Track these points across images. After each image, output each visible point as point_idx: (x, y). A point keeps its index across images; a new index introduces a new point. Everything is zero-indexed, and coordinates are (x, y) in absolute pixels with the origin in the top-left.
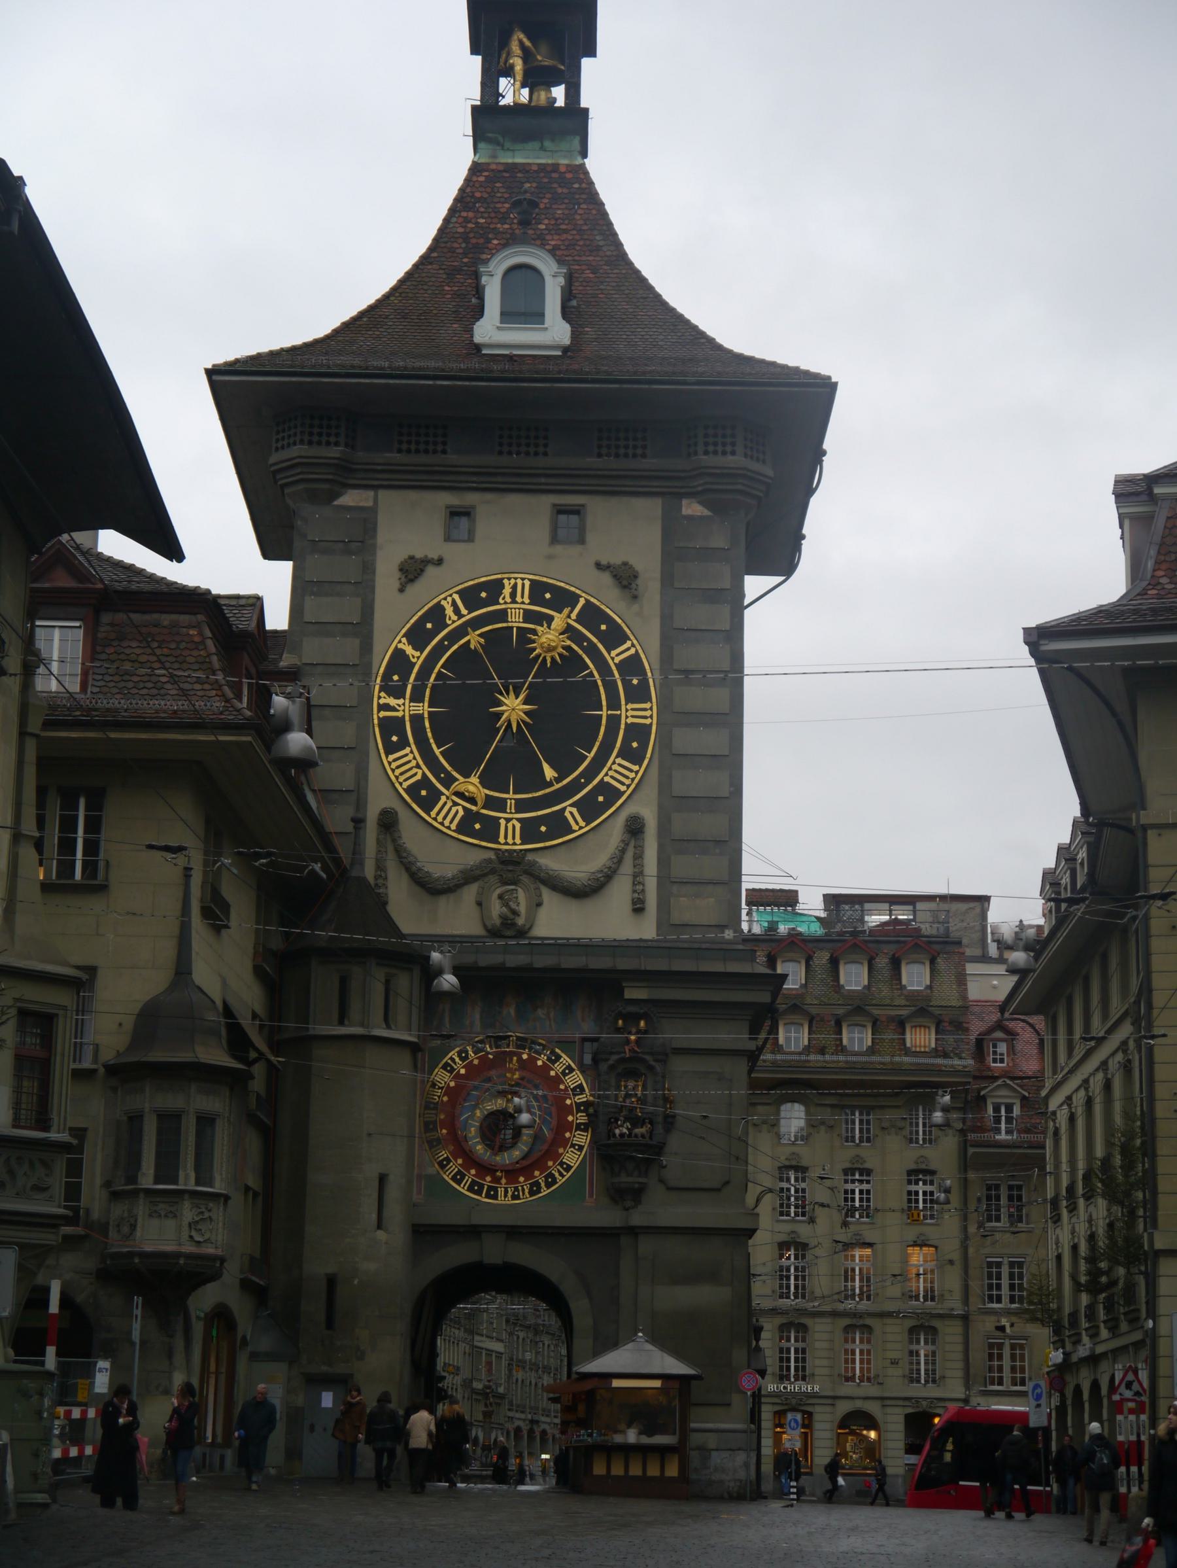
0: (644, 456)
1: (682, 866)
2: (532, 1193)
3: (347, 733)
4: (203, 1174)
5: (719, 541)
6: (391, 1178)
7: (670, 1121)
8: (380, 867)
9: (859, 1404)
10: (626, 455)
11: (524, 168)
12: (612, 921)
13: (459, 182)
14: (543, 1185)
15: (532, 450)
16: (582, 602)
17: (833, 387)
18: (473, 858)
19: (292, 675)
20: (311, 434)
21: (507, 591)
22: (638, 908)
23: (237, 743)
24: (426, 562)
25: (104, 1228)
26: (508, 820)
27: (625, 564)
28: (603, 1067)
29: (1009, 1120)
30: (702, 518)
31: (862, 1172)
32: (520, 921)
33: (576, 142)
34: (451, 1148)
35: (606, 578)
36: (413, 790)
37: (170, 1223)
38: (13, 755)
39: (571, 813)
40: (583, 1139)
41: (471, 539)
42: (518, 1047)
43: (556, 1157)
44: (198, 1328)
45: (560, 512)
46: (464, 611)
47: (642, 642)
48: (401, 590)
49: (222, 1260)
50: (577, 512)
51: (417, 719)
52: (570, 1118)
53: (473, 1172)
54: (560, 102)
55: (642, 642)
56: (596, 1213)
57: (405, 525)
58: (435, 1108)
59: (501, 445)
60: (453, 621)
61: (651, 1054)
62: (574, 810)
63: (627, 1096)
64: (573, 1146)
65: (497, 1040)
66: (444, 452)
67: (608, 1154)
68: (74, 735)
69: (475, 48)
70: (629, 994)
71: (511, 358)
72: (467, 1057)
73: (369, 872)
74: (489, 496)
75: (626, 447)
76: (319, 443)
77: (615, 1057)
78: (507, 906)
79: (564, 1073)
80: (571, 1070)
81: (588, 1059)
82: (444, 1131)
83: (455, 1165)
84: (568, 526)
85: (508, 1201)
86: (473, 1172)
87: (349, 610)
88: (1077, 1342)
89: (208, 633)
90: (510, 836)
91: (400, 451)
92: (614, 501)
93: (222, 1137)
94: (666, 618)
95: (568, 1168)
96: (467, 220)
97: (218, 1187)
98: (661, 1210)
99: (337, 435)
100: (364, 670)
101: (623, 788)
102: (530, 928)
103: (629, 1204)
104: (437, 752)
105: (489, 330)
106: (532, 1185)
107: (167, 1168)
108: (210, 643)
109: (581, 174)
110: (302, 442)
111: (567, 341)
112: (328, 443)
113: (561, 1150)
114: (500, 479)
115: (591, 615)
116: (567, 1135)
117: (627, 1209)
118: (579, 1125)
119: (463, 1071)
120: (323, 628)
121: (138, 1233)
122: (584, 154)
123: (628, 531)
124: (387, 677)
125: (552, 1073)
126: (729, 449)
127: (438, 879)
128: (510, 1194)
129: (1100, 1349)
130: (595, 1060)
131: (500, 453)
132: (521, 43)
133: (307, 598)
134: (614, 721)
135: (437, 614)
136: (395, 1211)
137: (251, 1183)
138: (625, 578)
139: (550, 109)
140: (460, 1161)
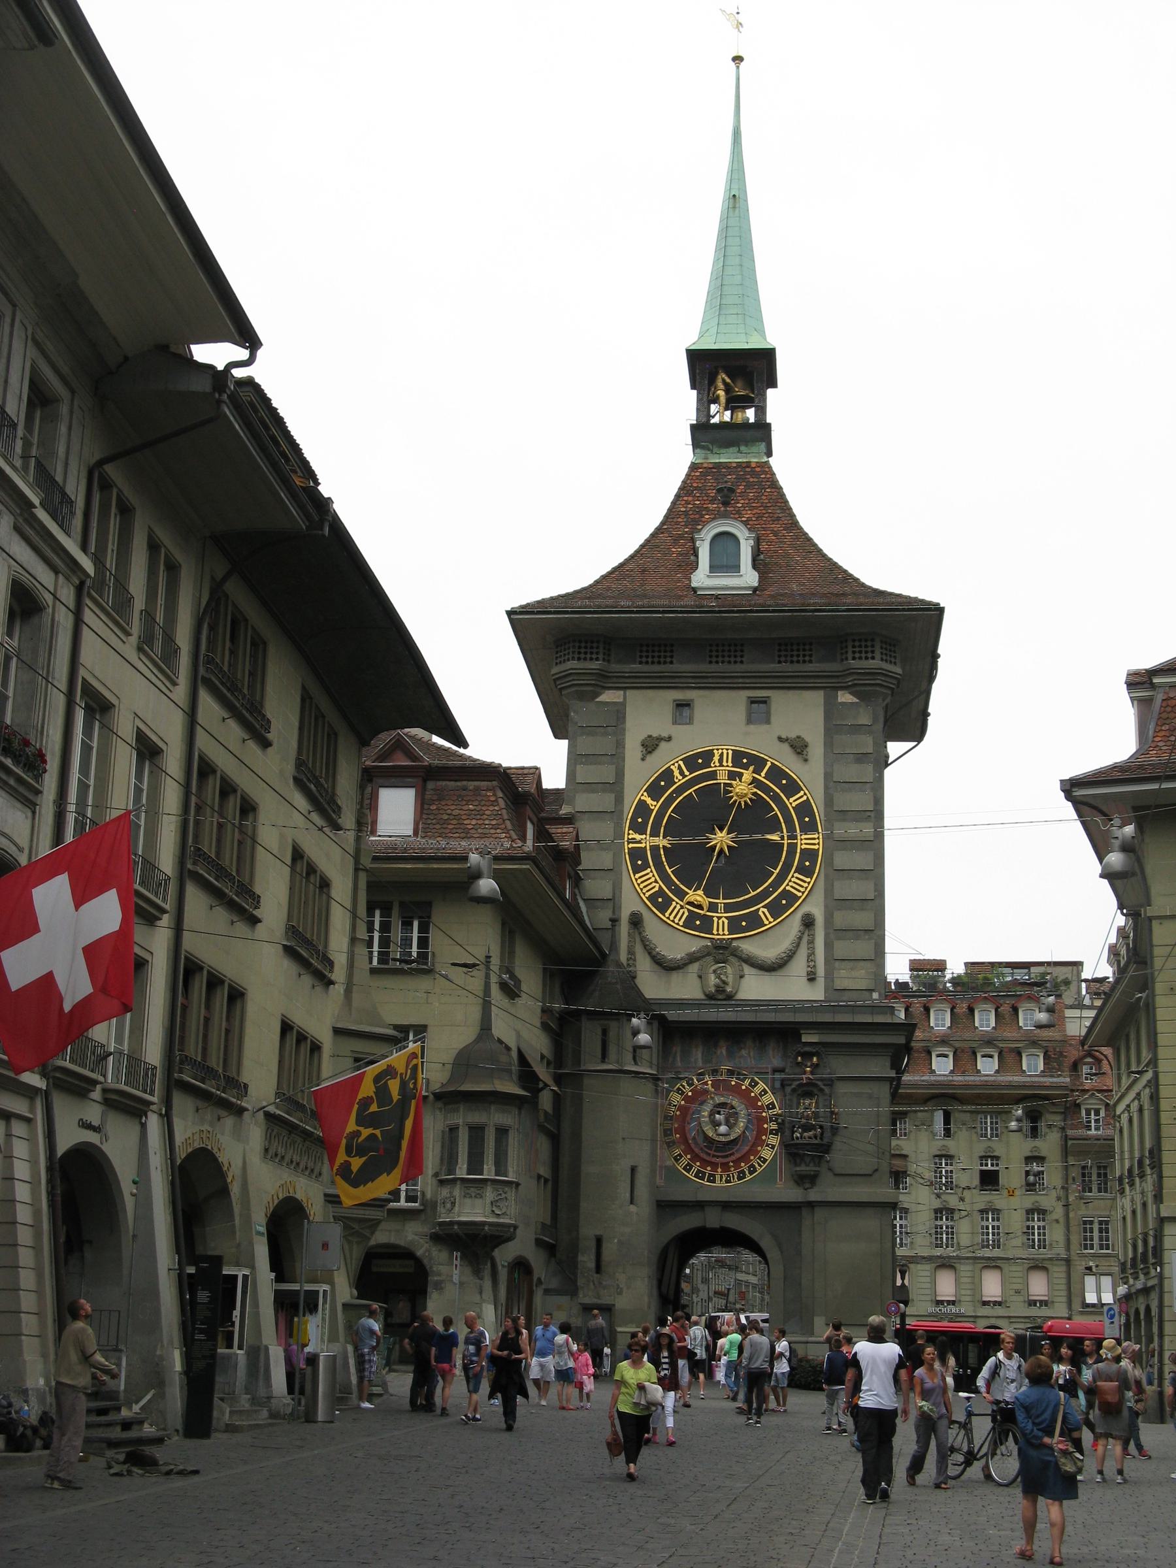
0: (810, 662)
1: (843, 948)
3: (606, 860)
4: (500, 1166)
5: (864, 719)
6: (640, 1169)
8: (631, 952)
9: (993, 1322)
10: (798, 662)
11: (726, 466)
12: (794, 988)
13: (682, 477)
15: (732, 659)
16: (769, 764)
17: (941, 611)
18: (694, 946)
19: (569, 820)
20: (579, 653)
21: (716, 758)
22: (812, 978)
23: (520, 870)
24: (660, 739)
25: (434, 1205)
26: (719, 918)
27: (799, 737)
28: (788, 1089)
29: (1097, 1121)
30: (852, 703)
31: (993, 1158)
32: (729, 989)
33: (763, 446)
35: (786, 746)
36: (652, 898)
37: (478, 1202)
38: (350, 885)
39: (763, 912)
40: (774, 1140)
41: (690, 721)
44: (503, 1275)
45: (752, 702)
46: (687, 773)
47: (812, 790)
48: (643, 759)
49: (515, 1227)
50: (765, 702)
51: (655, 849)
54: (752, 420)
55: (812, 790)
56: (784, 1191)
57: (646, 714)
59: (711, 656)
60: (679, 780)
62: (765, 910)
65: (715, 1072)
66: (671, 663)
67: (792, 1151)
68: (409, 866)
69: (693, 387)
71: (717, 597)
73: (623, 957)
74: (701, 692)
75: (798, 656)
76: (585, 659)
78: (719, 978)
80: (766, 1092)
81: (777, 1085)
84: (759, 711)
85: (722, 1185)
87: (606, 773)
88: (1136, 1278)
89: (500, 794)
90: (721, 929)
91: (641, 663)
92: (791, 693)
93: (513, 1141)
94: (828, 776)
96: (688, 503)
97: (511, 1178)
98: (829, 1190)
99: (597, 653)
100: (616, 814)
101: (799, 894)
103: (807, 1185)
104: (669, 871)
105: (702, 578)
107: (475, 1165)
108: (501, 802)
109: (766, 469)
110: (573, 659)
111: (756, 584)
112: (591, 659)
114: (710, 680)
115: (776, 774)
120: (589, 787)
121: (456, 1209)
122: (769, 454)
123: (800, 713)
124: (634, 819)
126: (870, 655)
127: (671, 960)
129: (1150, 1284)
130: (783, 1086)
131: (711, 662)
132: (724, 380)
133: (578, 767)
134: (792, 848)
135: (668, 775)
136: (642, 1191)
137: (542, 1173)
138: (799, 747)
139: (746, 425)
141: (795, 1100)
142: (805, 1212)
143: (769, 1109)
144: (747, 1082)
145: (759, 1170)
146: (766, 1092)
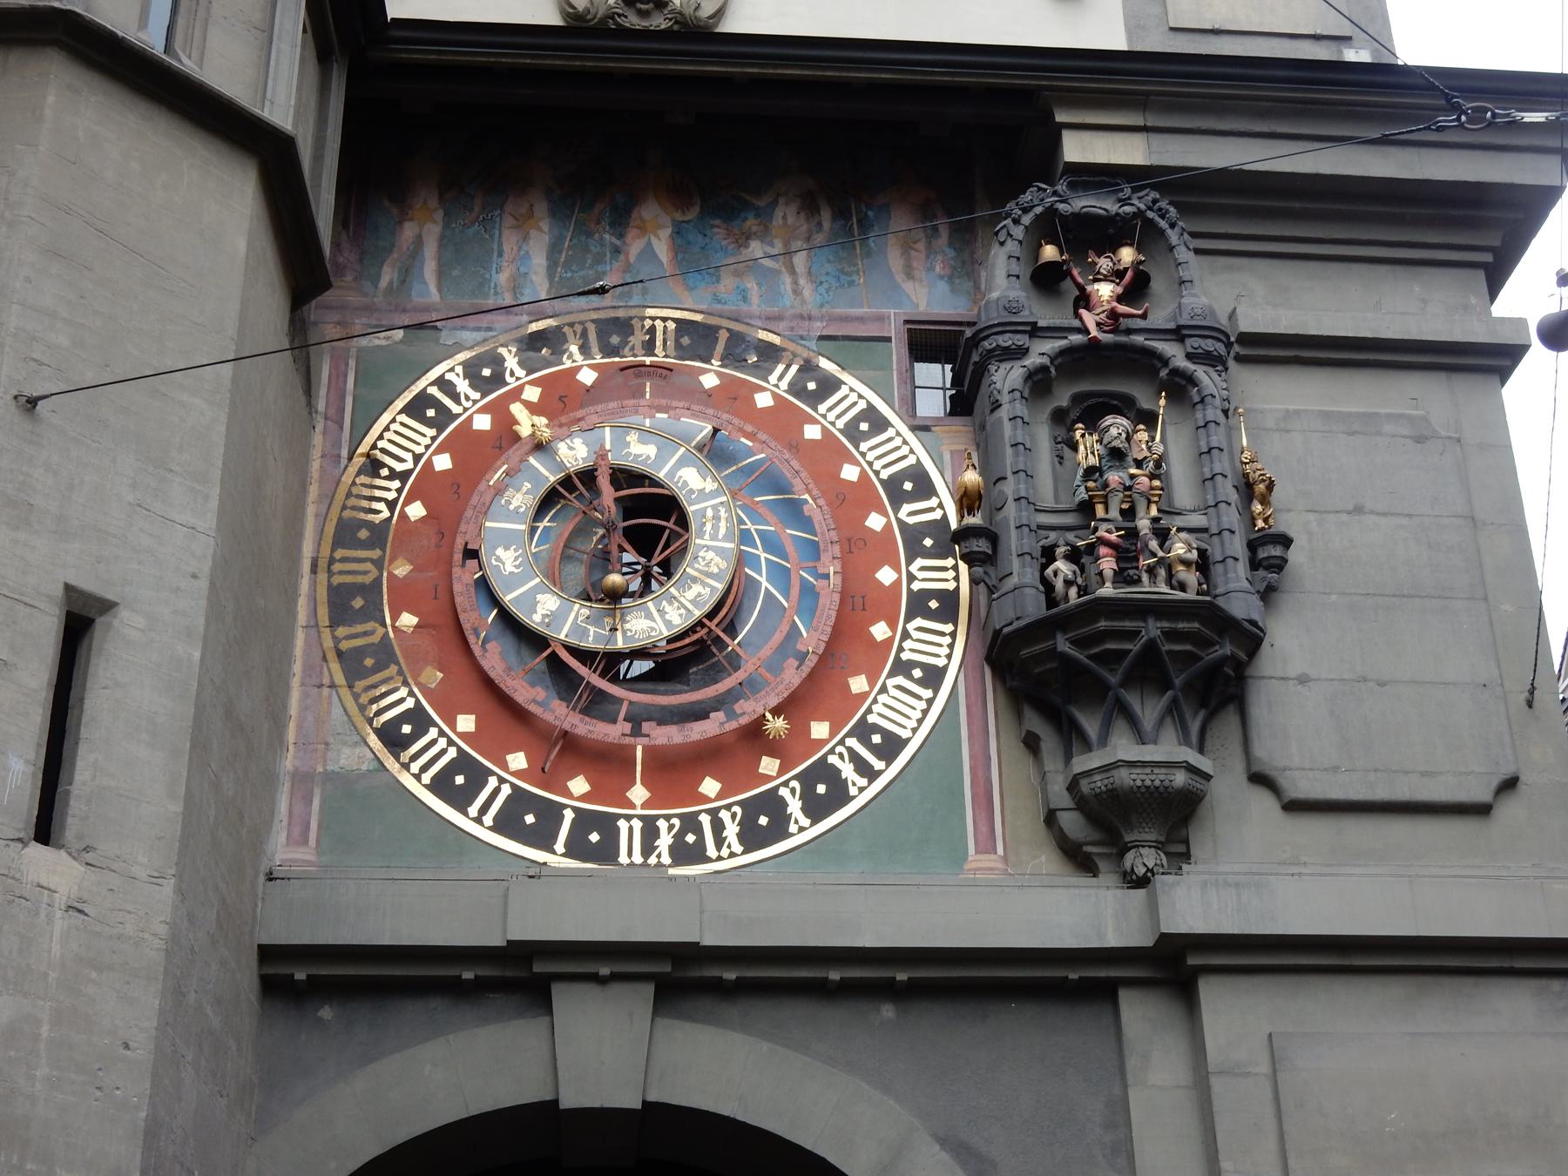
2: (752, 838)
7: (1268, 553)
14: (794, 806)
28: (1007, 378)
34: (434, 676)
40: (945, 647)
42: (682, 352)
43: (841, 707)
52: (886, 576)
53: (518, 761)
61: (1178, 334)
63: (1117, 455)
64: (903, 668)
70: (1077, 149)
77: (1041, 352)
79: (852, 431)
80: (880, 424)
81: (932, 404)
82: (408, 620)
83: (442, 744)
86: (518, 761)
95: (891, 747)
102: (720, 13)
103: (1144, 859)
113: (858, 684)
116: (880, 631)
117: (1142, 882)
118: (919, 603)
125: (812, 432)
128: (665, 841)
140: (466, 723)
141: (1043, 436)
142: (1139, 1013)
143: (898, 497)
144: (781, 378)
145: (862, 792)
146: (880, 424)
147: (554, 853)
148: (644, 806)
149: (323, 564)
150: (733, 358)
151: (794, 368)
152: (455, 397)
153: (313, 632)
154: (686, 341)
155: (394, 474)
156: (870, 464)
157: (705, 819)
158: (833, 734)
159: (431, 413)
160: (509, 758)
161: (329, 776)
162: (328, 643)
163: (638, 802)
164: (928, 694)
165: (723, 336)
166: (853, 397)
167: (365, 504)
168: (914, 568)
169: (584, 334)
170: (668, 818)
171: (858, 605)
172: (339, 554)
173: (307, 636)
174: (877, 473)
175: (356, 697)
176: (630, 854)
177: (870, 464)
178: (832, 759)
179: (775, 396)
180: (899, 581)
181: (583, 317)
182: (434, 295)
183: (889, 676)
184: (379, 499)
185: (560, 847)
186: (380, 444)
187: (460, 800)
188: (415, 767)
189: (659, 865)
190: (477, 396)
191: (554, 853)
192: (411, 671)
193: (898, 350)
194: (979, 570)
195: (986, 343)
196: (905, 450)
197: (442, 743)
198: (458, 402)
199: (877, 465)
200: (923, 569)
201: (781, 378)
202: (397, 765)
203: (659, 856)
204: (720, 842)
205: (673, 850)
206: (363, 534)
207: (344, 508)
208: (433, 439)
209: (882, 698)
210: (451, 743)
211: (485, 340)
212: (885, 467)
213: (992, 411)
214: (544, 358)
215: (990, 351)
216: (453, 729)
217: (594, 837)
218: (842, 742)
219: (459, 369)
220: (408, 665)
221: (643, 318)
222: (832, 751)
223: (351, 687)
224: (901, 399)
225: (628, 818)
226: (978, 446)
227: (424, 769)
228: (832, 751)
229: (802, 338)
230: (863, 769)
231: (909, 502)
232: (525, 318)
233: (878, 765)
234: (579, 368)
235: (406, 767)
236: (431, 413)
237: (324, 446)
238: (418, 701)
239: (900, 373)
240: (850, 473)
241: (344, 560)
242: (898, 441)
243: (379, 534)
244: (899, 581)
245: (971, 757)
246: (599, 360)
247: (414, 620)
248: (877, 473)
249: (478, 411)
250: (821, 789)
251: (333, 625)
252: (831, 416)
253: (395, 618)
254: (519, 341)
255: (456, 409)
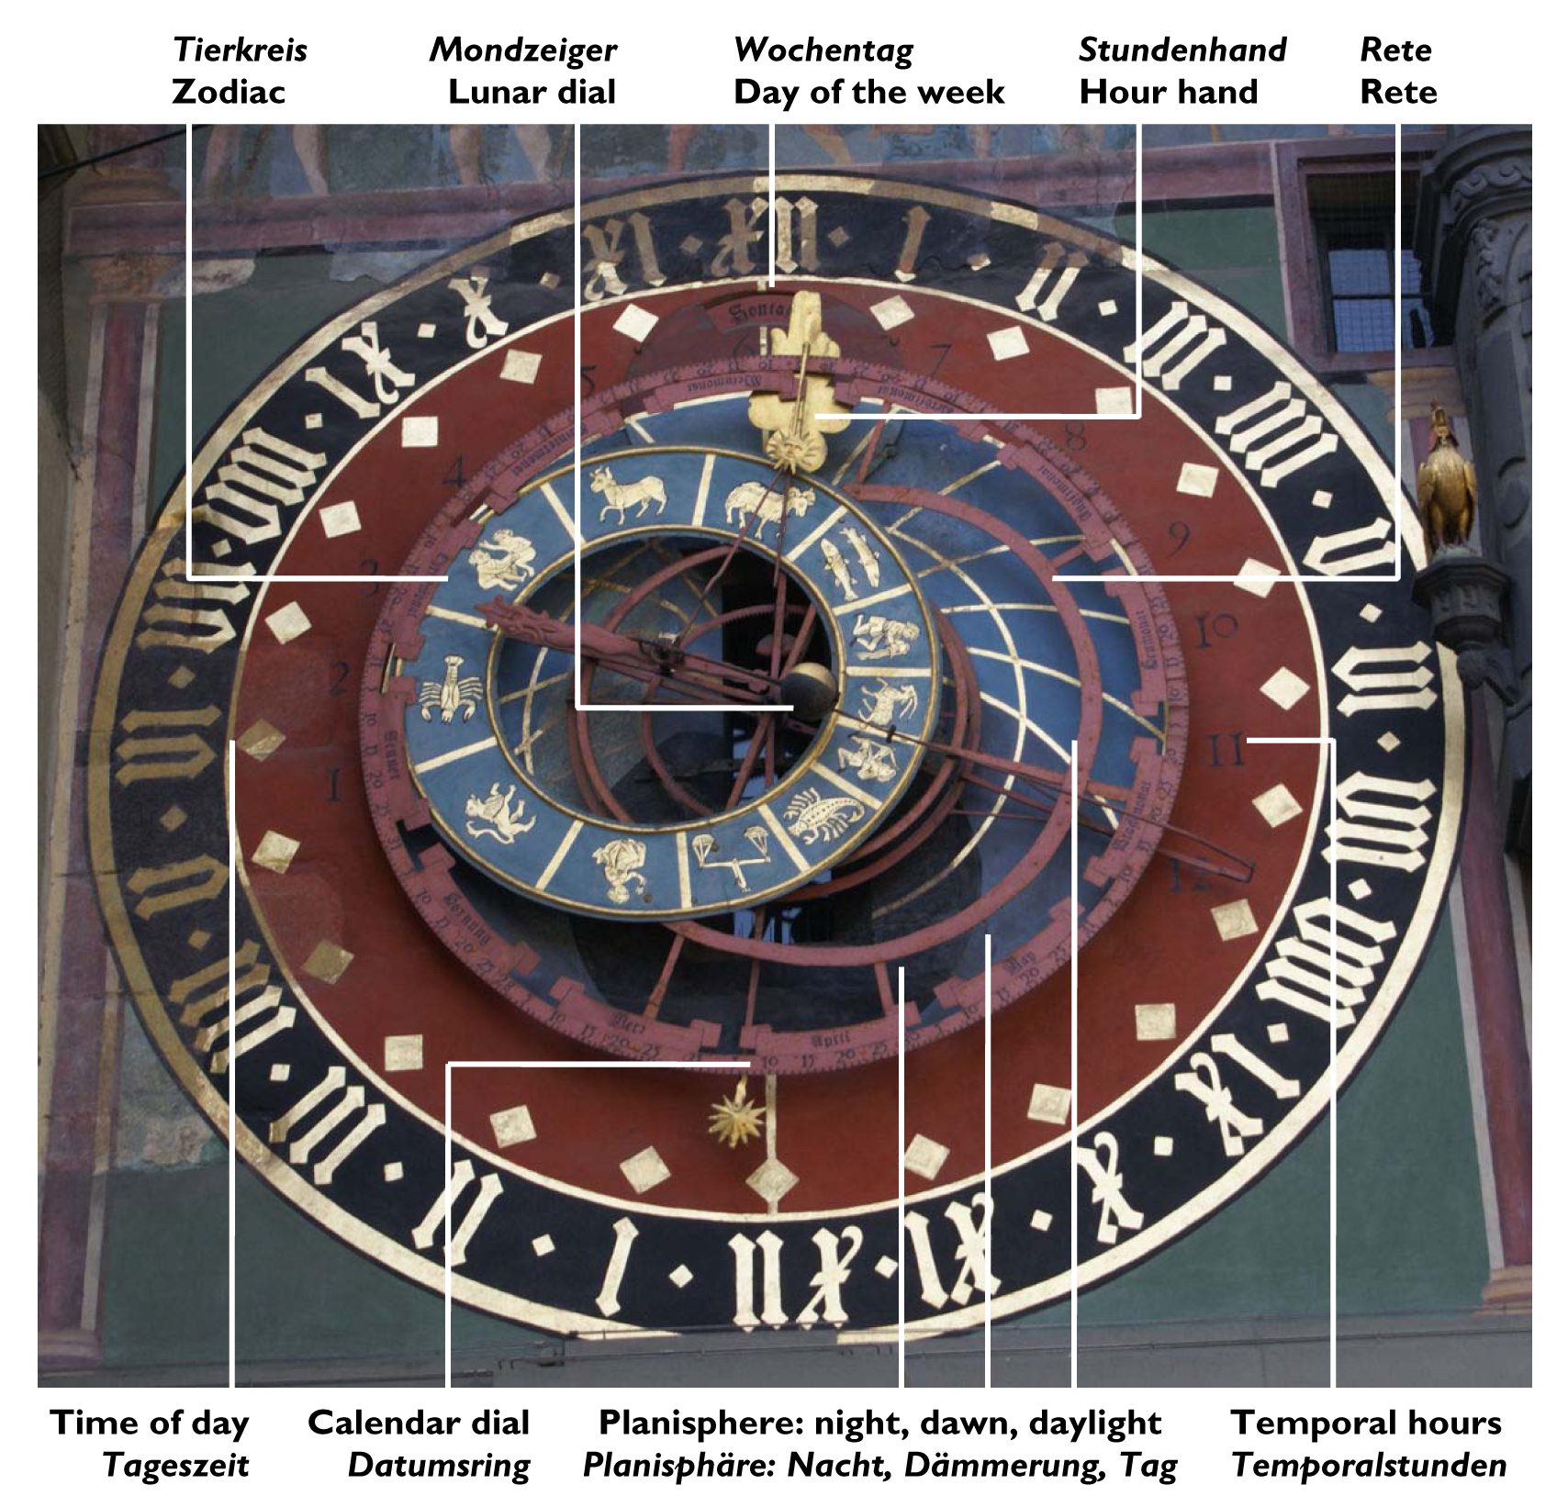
14: (1108, 1187)
34: (332, 960)
43: (1197, 971)
52: (1284, 688)
58: (192, 699)
72: (451, 344)
79: (1197, 394)
80: (1254, 375)
82: (278, 848)
106: (1015, 1197)
113: (1233, 921)
119: (422, 433)
128: (831, 1277)
144: (1042, 298)
146: (1254, 375)
147: (597, 1313)
148: (784, 1205)
149: (99, 742)
150: (940, 262)
151: (1070, 275)
152: (364, 387)
153: (83, 884)
154: (839, 236)
155: (242, 552)
156: (1239, 459)
157: (917, 1226)
158: (1183, 1029)
159: (314, 421)
160: (497, 1119)
161: (121, 1181)
162: (114, 906)
163: (772, 1198)
164: (1384, 931)
165: (918, 221)
166: (1198, 325)
167: (184, 615)
168: (1342, 669)
169: (628, 239)
170: (836, 1226)
171: (1225, 751)
172: (133, 721)
173: (69, 891)
174: (1254, 477)
175: (174, 1011)
176: (758, 1307)
177: (1239, 459)
178: (1185, 1082)
179: (1029, 332)
180: (1312, 696)
181: (623, 203)
182: (318, 186)
183: (1298, 900)
184: (212, 605)
185: (608, 1301)
186: (211, 493)
187: (397, 1214)
188: (300, 1151)
189: (823, 1326)
190: (407, 380)
191: (597, 1313)
192: (285, 952)
193: (1285, 229)
194: (1477, 656)
195: (1465, 185)
196: (1313, 425)
197: (356, 1096)
198: (371, 396)
199: (1255, 461)
200: (1360, 669)
201: (1041, 297)
202: (262, 1150)
203: (820, 1308)
204: (949, 1270)
205: (845, 1289)
206: (182, 677)
207: (141, 626)
208: (321, 474)
209: (1288, 947)
210: (373, 1096)
211: (422, 267)
212: (1270, 463)
213: (1488, 322)
214: (546, 293)
215: (1474, 198)
216: (377, 1063)
217: (681, 1276)
218: (1203, 1045)
219: (370, 330)
220: (281, 938)
221: (748, 198)
222: (1183, 1066)
223: (162, 991)
224: (1299, 321)
225: (753, 1232)
226: (1467, 403)
227: (319, 1153)
228: (1183, 1066)
229: (1083, 211)
230: (1251, 1097)
231: (1326, 533)
232: (504, 216)
233: (1285, 1088)
234: (619, 309)
235: (281, 1151)
236: (314, 421)
237: (97, 501)
238: (302, 1015)
239: (1293, 267)
240: (1197, 481)
241: (143, 733)
242: (1297, 409)
243: (214, 674)
244: (1312, 696)
245: (1486, 1059)
246: (659, 288)
247: (292, 847)
248: (1254, 477)
249: (417, 410)
250: (1163, 1146)
251: (126, 862)
252: (1153, 367)
253: (249, 845)
254: (491, 262)
255: (365, 409)
